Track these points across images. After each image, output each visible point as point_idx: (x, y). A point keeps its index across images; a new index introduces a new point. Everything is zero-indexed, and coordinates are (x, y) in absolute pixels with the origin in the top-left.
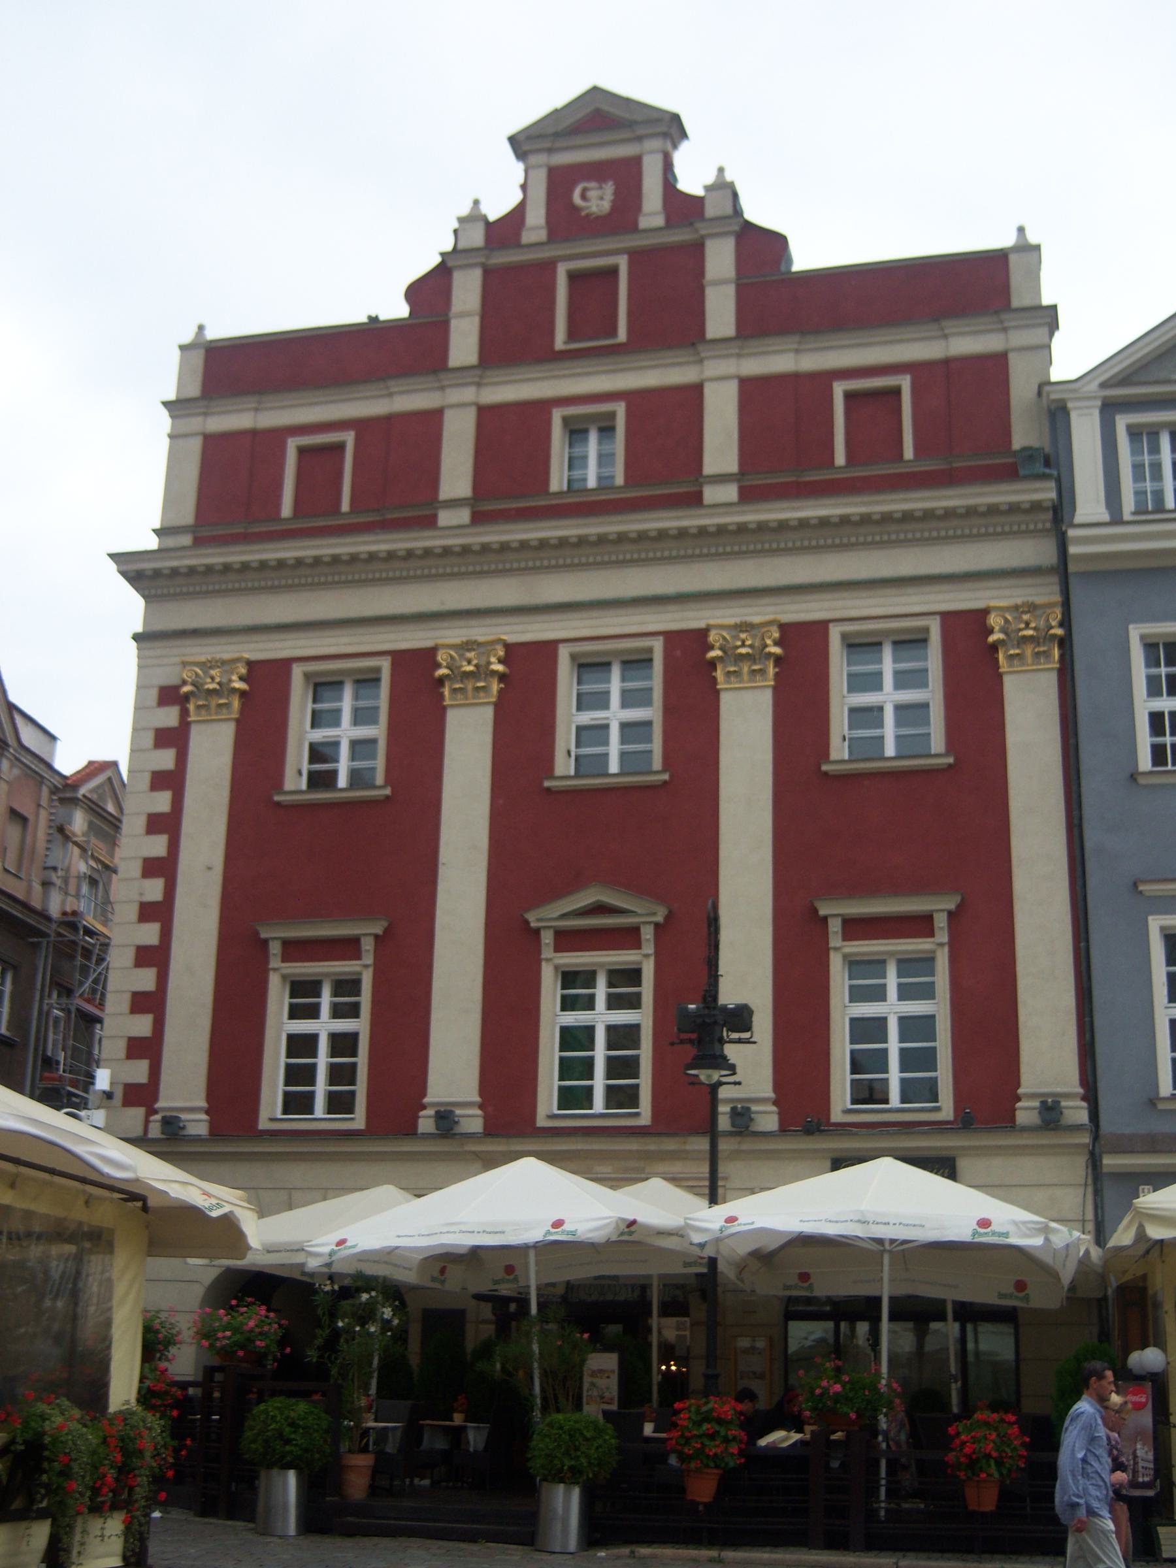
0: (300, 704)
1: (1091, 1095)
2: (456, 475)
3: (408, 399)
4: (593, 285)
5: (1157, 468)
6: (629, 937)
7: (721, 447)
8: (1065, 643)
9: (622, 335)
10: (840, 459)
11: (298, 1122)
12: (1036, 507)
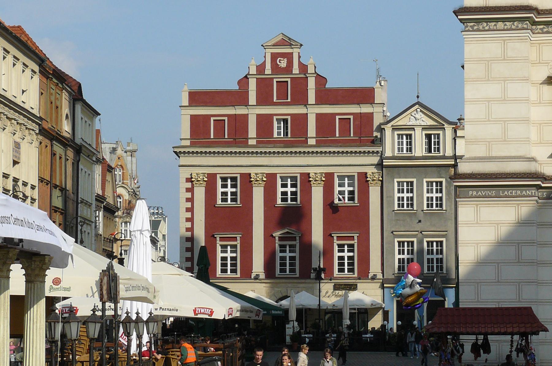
0: (219, 183)
1: (383, 273)
2: (252, 131)
3: (240, 111)
4: (282, 85)
5: (402, 142)
6: (294, 239)
7: (312, 130)
8: (382, 181)
9: (289, 100)
10: (337, 135)
11: (224, 275)
12: (378, 152)
